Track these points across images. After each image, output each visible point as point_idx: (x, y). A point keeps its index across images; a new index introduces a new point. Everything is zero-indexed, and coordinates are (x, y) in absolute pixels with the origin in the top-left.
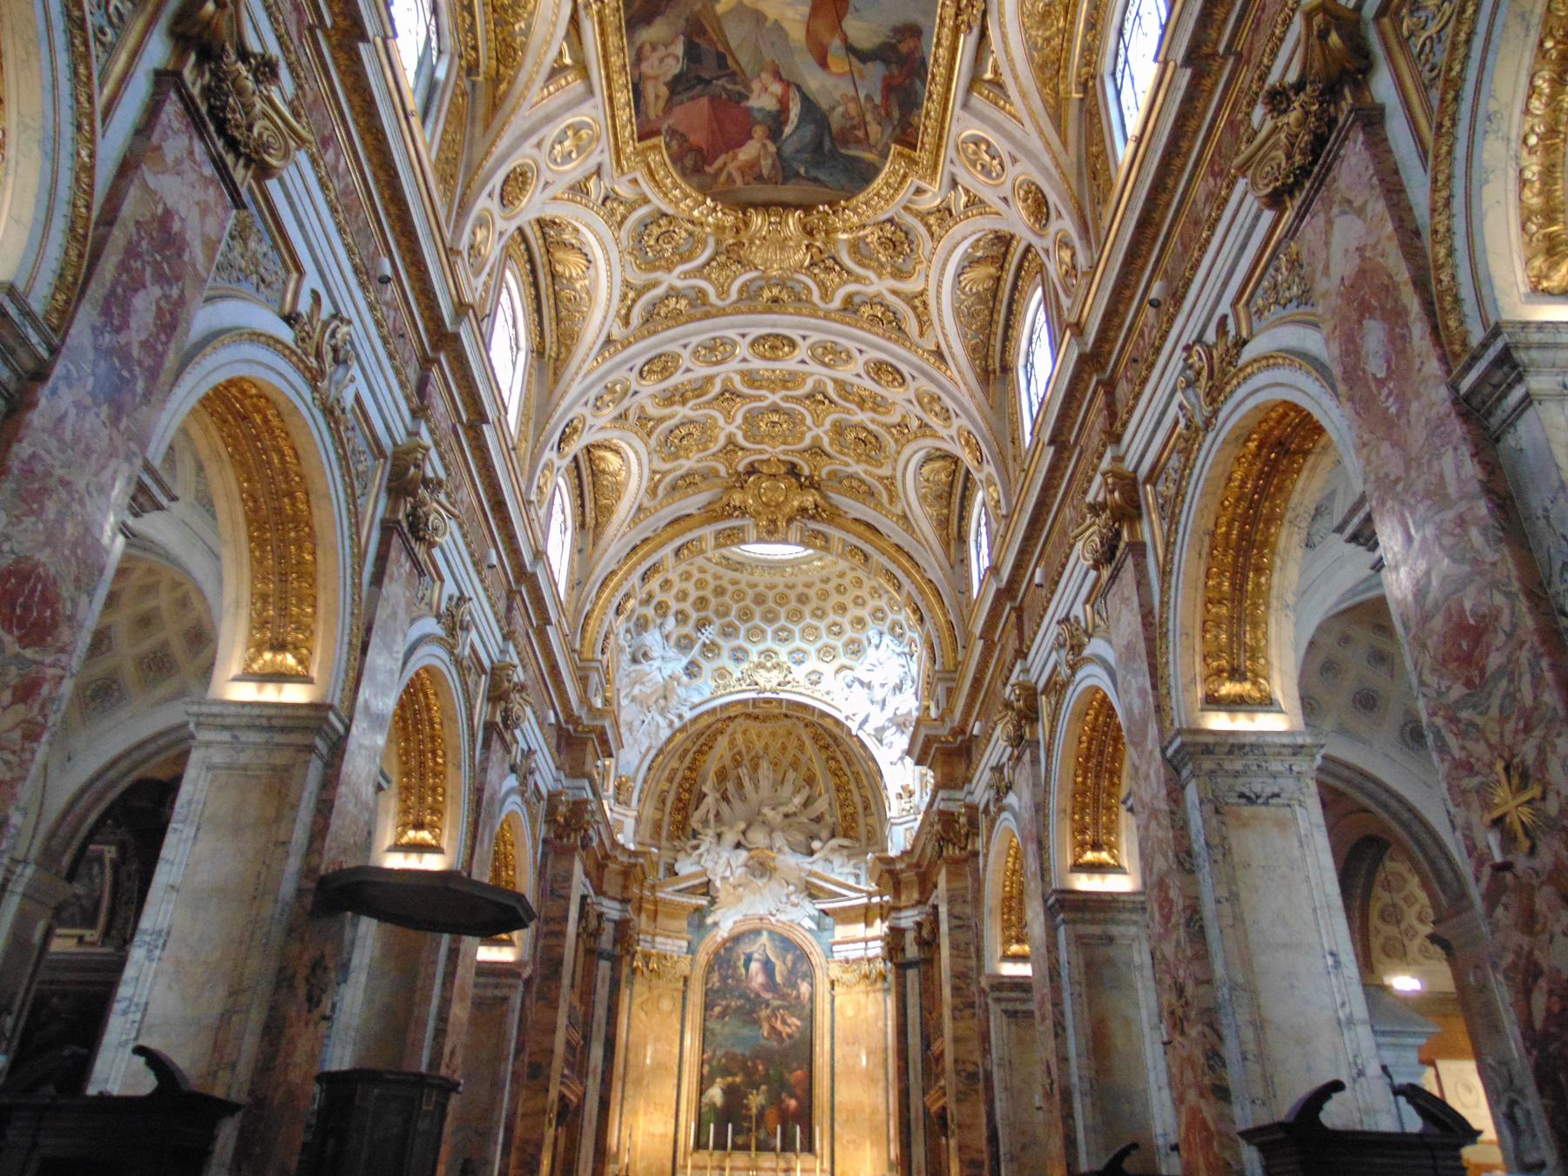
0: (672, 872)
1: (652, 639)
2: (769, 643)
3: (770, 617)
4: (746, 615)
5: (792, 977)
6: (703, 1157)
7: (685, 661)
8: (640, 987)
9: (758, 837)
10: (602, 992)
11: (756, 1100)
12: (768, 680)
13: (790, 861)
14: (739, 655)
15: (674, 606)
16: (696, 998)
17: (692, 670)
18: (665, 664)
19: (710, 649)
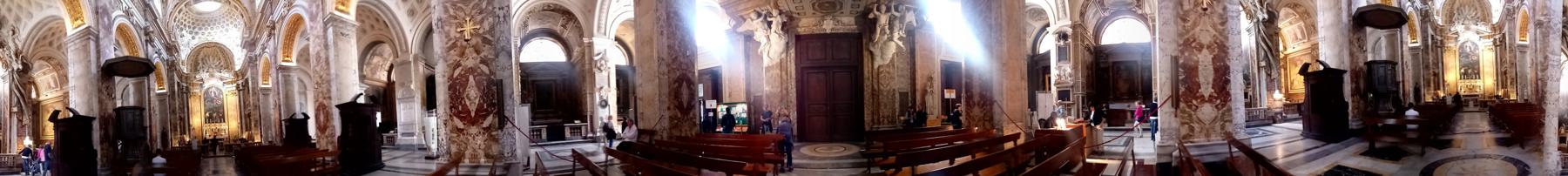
0: (195, 77)
1: (184, 32)
2: (209, 31)
3: (209, 25)
4: (204, 25)
5: (219, 94)
6: (208, 125)
7: (191, 36)
8: (192, 98)
9: (211, 70)
10: (185, 98)
11: (215, 115)
12: (210, 39)
13: (217, 74)
14: (203, 34)
15: (188, 25)
16: (202, 100)
17: (193, 38)
18: (188, 37)
19: (197, 33)
